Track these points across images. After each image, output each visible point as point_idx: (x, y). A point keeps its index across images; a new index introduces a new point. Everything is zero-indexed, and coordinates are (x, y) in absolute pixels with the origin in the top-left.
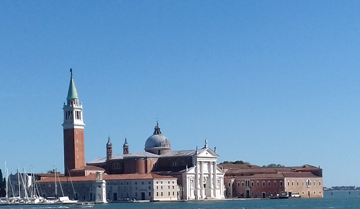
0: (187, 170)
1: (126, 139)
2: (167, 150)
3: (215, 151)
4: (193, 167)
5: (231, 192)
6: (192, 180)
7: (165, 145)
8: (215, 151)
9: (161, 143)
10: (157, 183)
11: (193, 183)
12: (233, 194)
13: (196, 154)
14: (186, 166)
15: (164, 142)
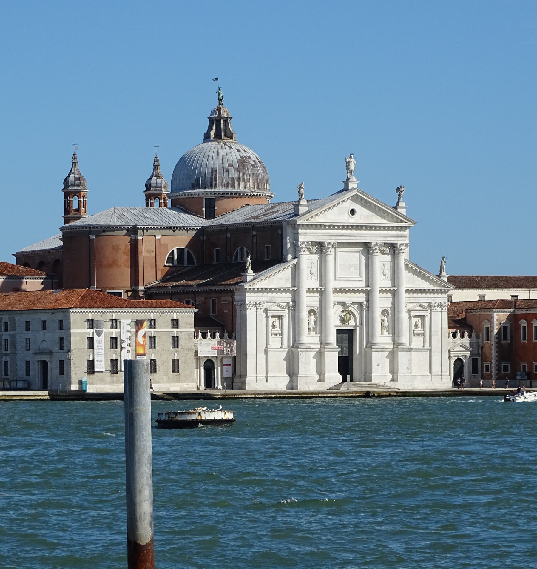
0: (249, 278)
1: (156, 160)
2: (246, 201)
3: (398, 201)
4: (285, 265)
5: (491, 363)
6: (273, 316)
7: (233, 179)
8: (398, 201)
9: (216, 171)
10: (91, 324)
11: (281, 326)
12: (499, 370)
13: (297, 214)
14: (245, 263)
15: (232, 169)
